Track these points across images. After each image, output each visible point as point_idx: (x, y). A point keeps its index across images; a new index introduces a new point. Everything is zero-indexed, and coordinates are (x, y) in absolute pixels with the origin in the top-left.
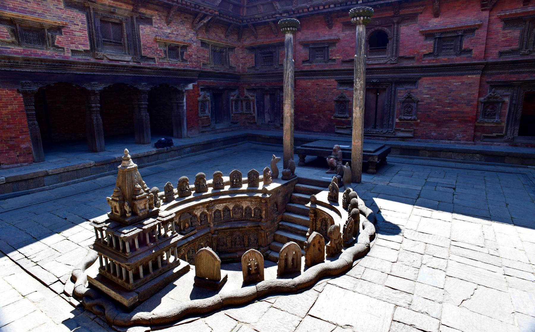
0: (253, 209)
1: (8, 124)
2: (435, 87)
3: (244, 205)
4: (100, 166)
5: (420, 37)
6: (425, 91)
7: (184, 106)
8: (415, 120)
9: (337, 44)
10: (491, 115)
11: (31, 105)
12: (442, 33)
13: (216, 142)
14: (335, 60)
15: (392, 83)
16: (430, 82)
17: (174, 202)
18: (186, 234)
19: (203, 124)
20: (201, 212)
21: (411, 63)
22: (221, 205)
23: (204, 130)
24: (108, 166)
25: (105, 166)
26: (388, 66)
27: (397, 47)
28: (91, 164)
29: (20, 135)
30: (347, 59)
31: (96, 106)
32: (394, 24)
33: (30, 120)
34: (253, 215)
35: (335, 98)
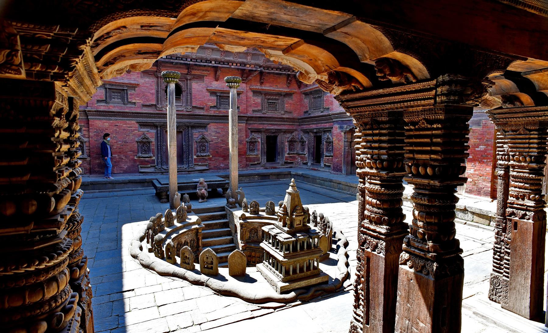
2: (220, 131)
5: (207, 93)
6: (213, 134)
8: (209, 156)
9: (136, 89)
10: (252, 150)
12: (221, 93)
14: (135, 103)
15: (188, 127)
16: (216, 127)
21: (202, 112)
26: (184, 113)
27: (191, 99)
30: (148, 104)
32: (187, 80)
35: (136, 139)
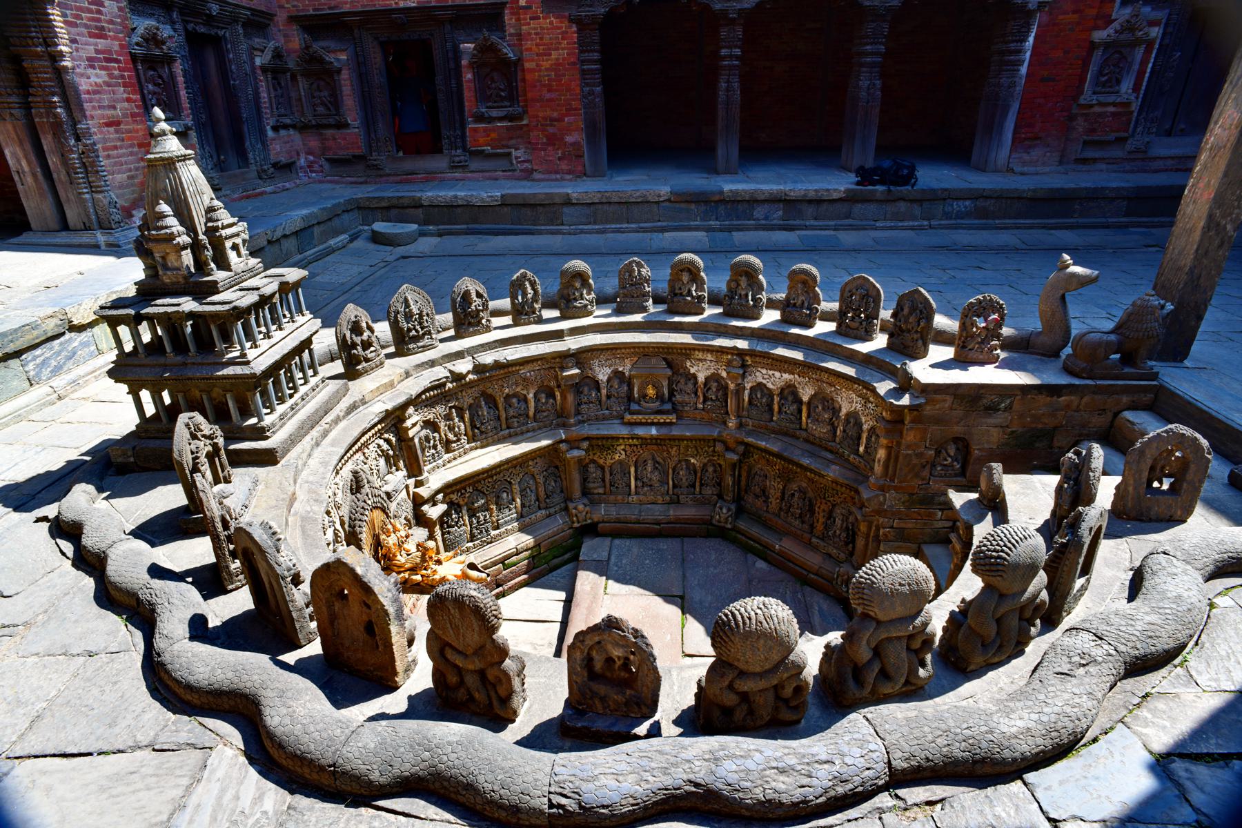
0: (865, 427)
1: (549, 91)
3: (848, 402)
4: (683, 205)
7: (1021, 62)
11: (592, 51)
13: (1093, 197)
17: (638, 317)
18: (638, 413)
19: (1092, 131)
20: (709, 373)
22: (777, 374)
23: (1090, 154)
24: (703, 208)
25: (693, 206)
28: (659, 196)
29: (567, 115)
31: (731, 53)
33: (587, 85)
34: (861, 449)
